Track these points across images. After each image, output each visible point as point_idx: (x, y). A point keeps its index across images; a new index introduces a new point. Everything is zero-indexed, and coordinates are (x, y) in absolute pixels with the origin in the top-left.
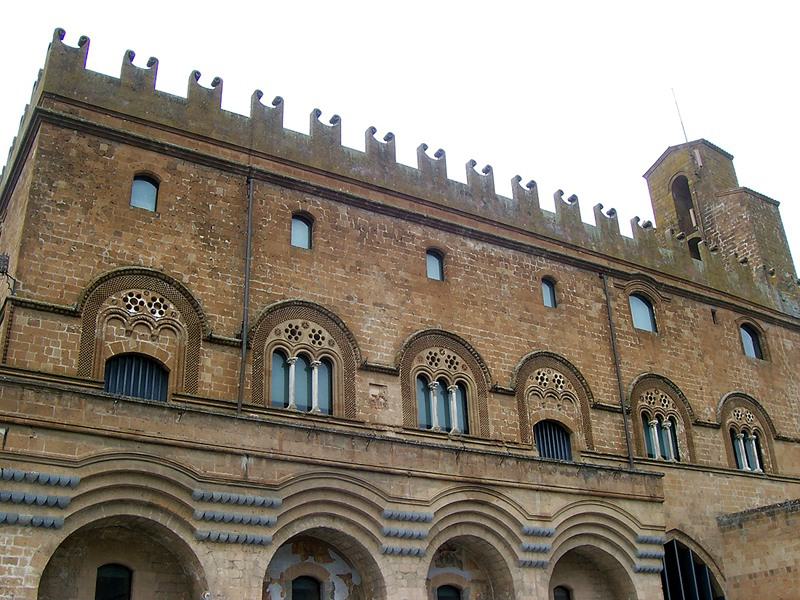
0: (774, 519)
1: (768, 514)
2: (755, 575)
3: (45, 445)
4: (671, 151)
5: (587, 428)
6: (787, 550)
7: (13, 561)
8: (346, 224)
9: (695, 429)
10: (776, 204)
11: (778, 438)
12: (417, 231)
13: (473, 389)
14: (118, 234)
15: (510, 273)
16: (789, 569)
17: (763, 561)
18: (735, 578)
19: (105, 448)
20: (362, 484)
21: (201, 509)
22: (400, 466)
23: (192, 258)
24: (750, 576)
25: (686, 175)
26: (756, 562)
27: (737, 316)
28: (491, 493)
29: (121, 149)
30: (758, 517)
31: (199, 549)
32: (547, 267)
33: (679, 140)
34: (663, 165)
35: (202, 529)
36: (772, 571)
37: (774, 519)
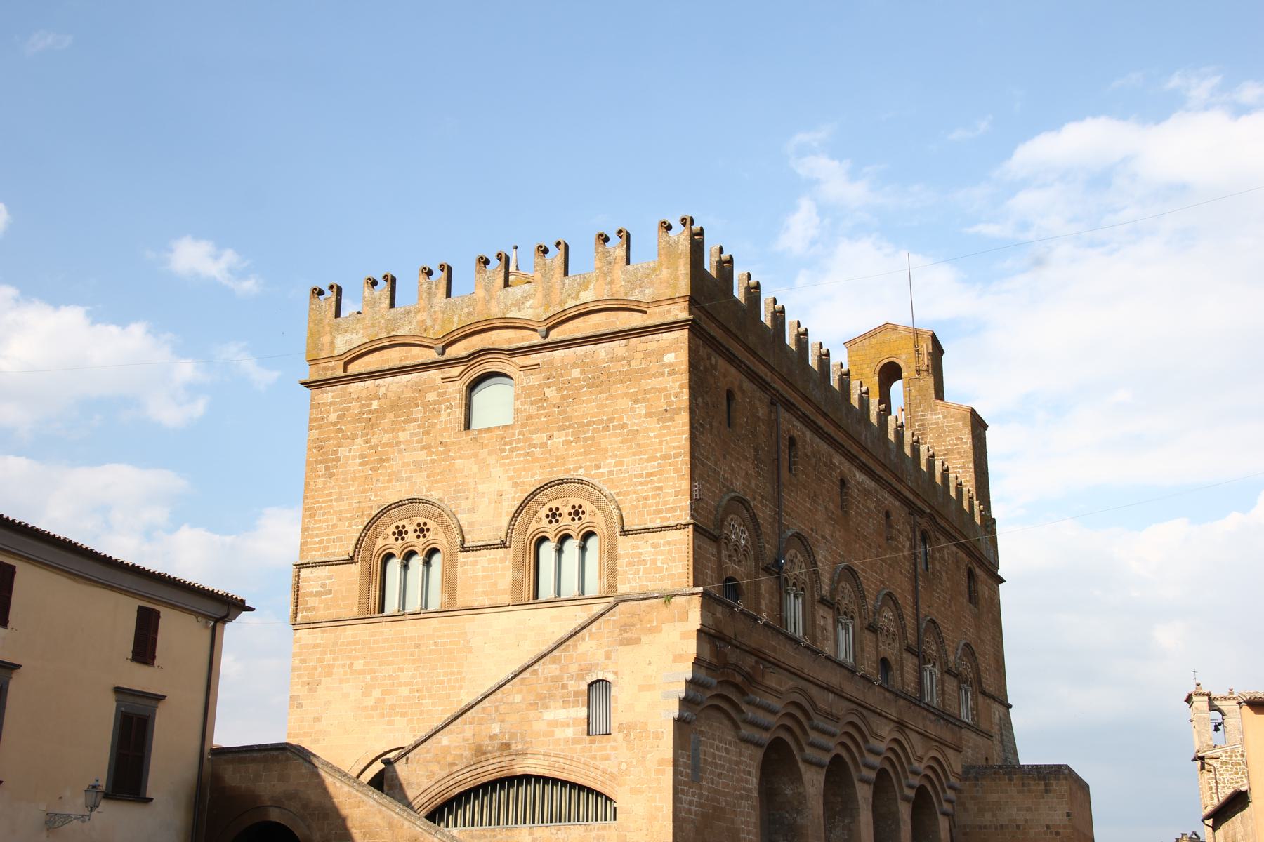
0: (1011, 779)
1: (1005, 774)
2: (985, 827)
3: (772, 680)
4: (885, 327)
5: (902, 670)
6: (1019, 809)
7: (749, 773)
8: (809, 451)
9: (946, 677)
10: (985, 427)
11: (983, 693)
12: (837, 459)
13: (857, 619)
14: (725, 457)
15: (872, 506)
16: (1018, 827)
17: (994, 816)
18: (965, 826)
19: (791, 683)
20: (863, 718)
21: (814, 736)
22: (879, 708)
23: (753, 482)
24: (980, 827)
25: (902, 364)
26: (988, 815)
27: (967, 559)
28: (902, 732)
29: (721, 363)
30: (995, 773)
31: (802, 766)
32: (889, 500)
33: (903, 319)
34: (873, 340)
35: (809, 752)
36: (1002, 826)
37: (1011, 779)
